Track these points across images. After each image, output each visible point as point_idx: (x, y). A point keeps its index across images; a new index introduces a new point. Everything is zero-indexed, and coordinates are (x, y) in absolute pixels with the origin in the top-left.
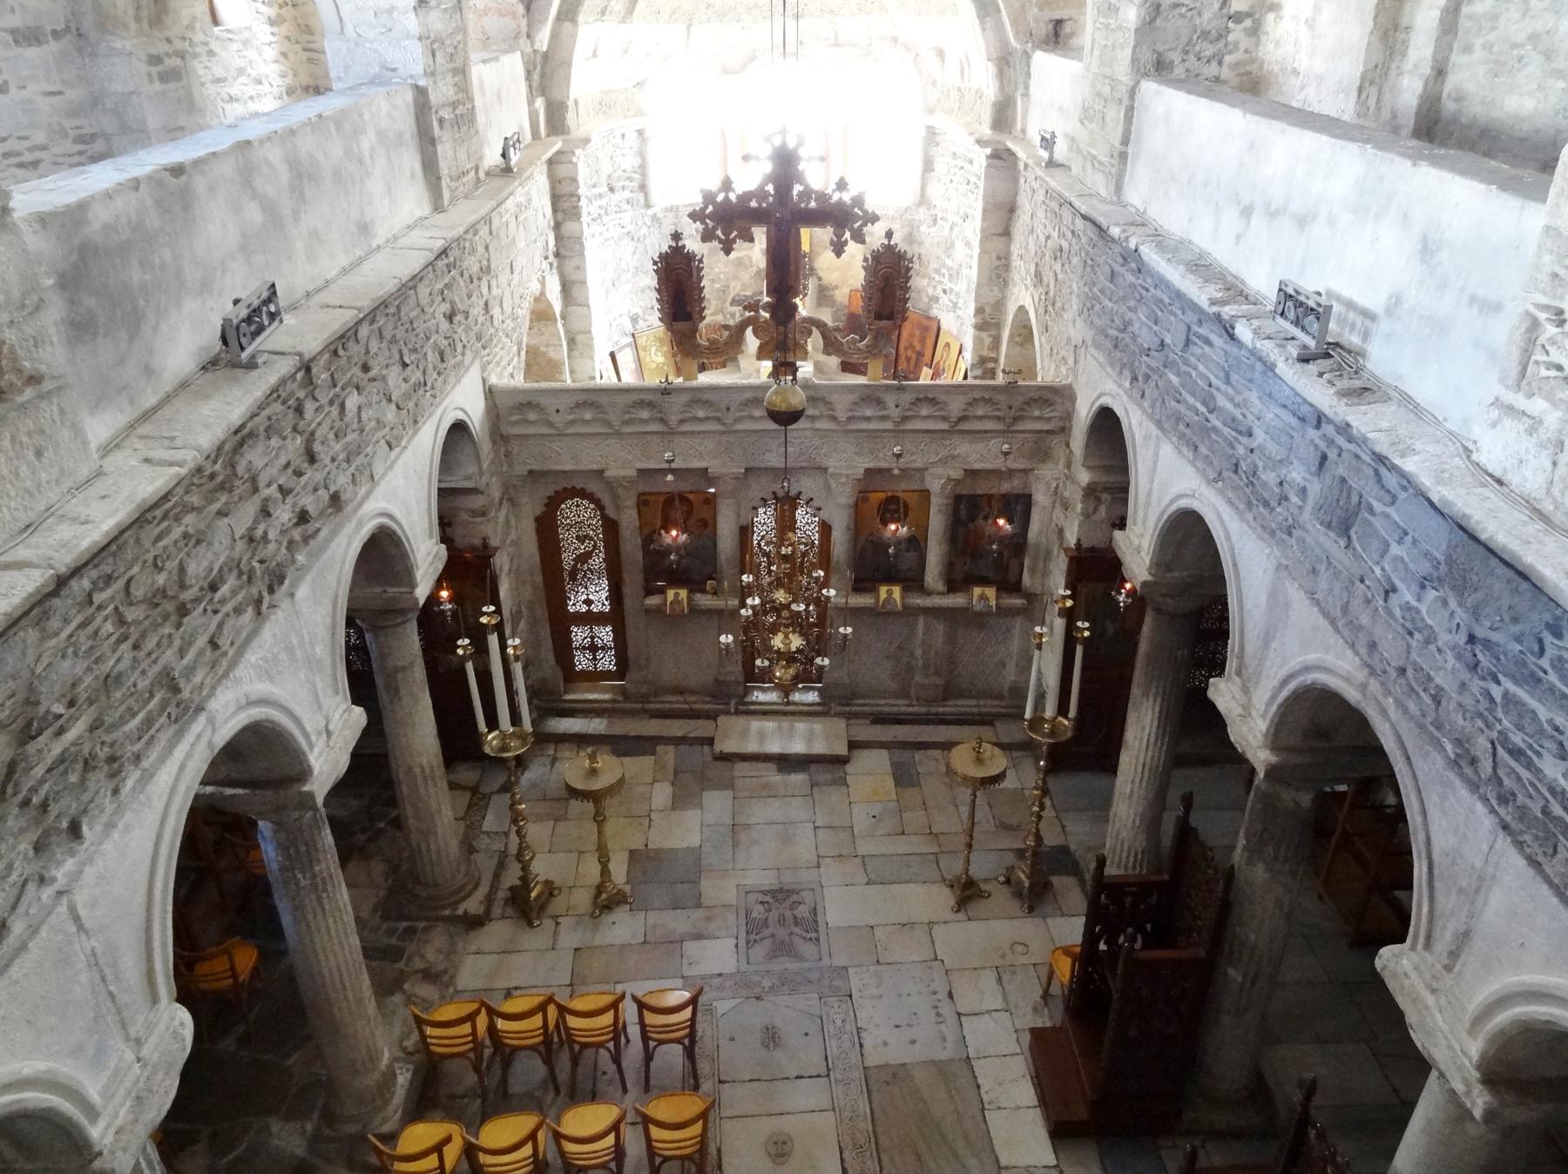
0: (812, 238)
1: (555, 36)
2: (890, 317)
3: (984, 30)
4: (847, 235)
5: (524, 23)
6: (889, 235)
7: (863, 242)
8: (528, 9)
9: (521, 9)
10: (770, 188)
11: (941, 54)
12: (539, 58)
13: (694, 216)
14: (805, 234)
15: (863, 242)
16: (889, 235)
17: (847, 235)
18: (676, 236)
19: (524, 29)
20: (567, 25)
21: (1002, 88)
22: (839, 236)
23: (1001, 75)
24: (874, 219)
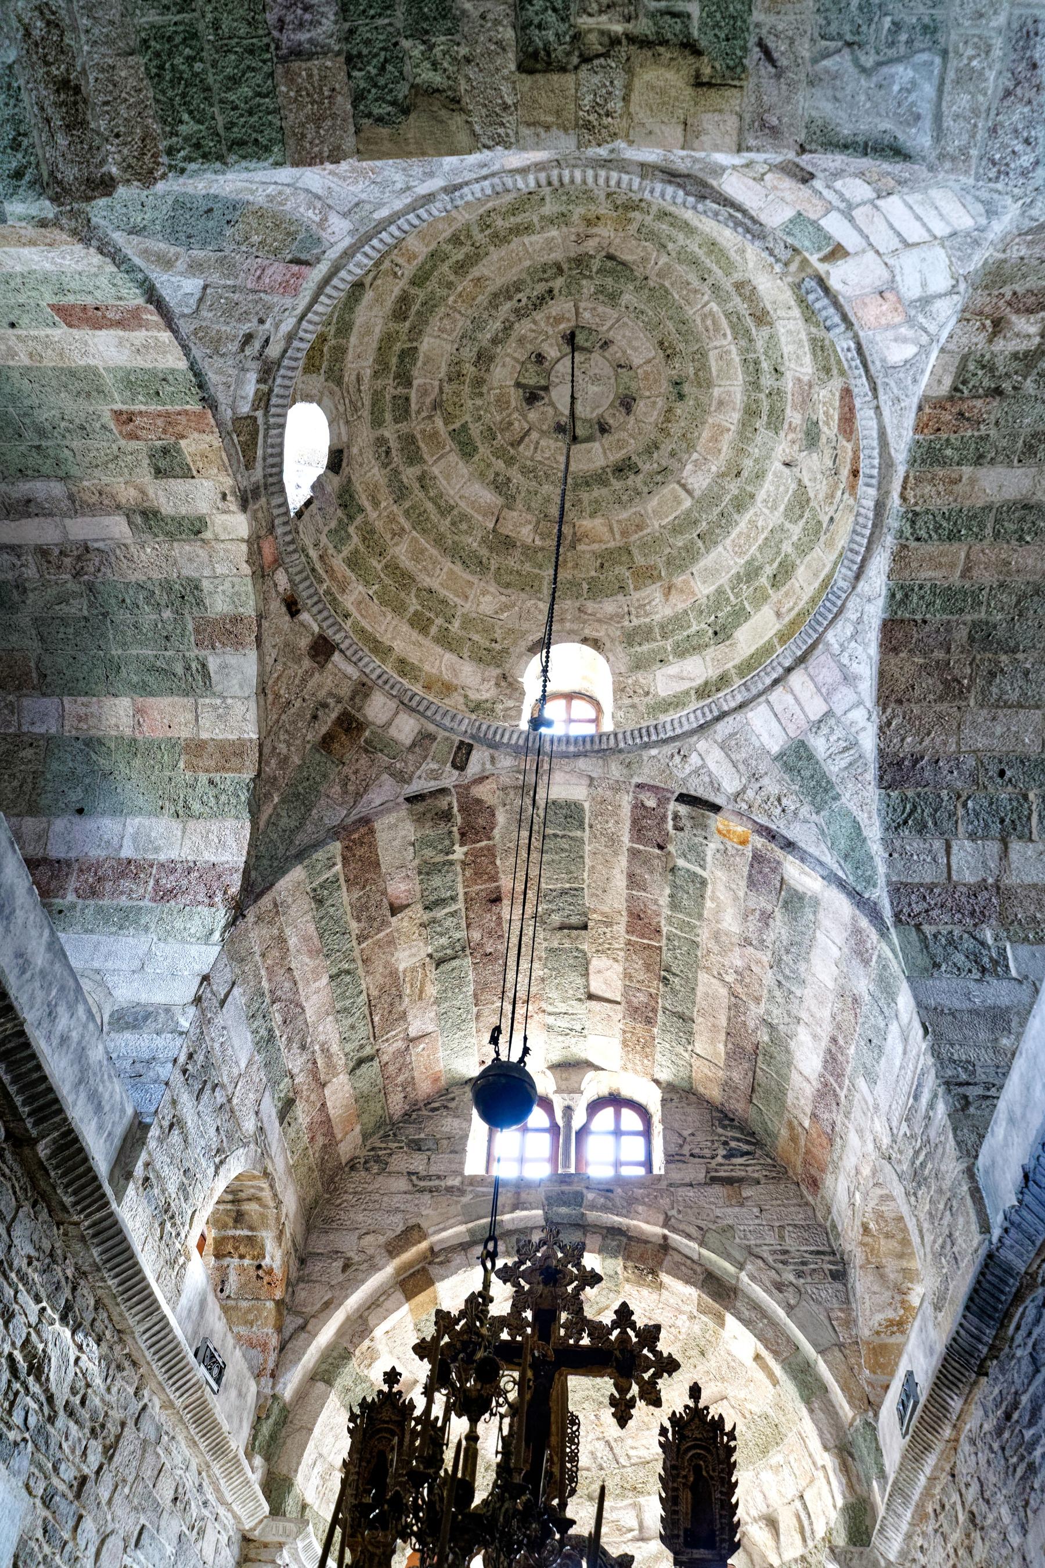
0: (587, 1395)
1: (302, 1395)
2: (709, 1543)
3: (811, 1411)
4: (635, 1389)
5: (273, 1357)
6: (695, 1391)
7: (657, 1402)
8: (282, 1348)
9: (274, 1341)
10: (528, 1315)
11: (772, 1523)
12: (276, 1410)
13: (421, 1350)
14: (574, 1382)
15: (657, 1402)
16: (695, 1391)
17: (635, 1389)
18: (392, 1377)
19: (271, 1365)
20: (321, 1386)
21: (850, 1486)
22: (623, 1389)
23: (845, 1469)
24: (670, 1366)
